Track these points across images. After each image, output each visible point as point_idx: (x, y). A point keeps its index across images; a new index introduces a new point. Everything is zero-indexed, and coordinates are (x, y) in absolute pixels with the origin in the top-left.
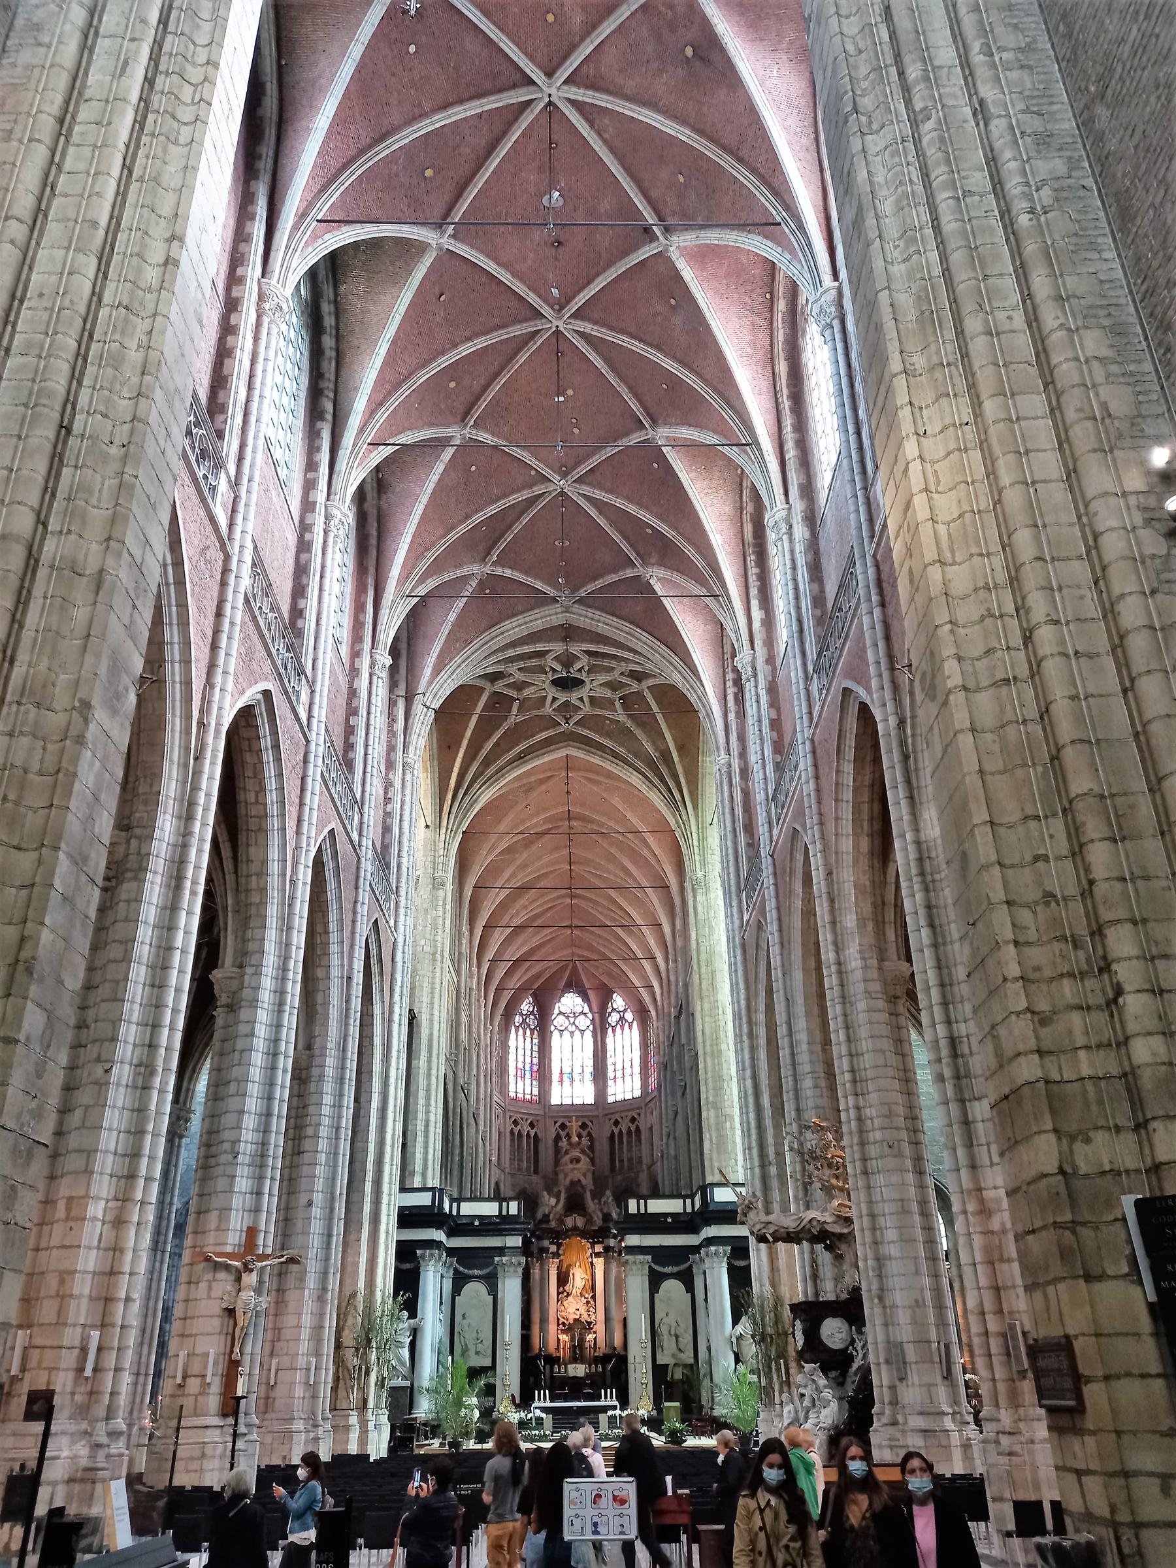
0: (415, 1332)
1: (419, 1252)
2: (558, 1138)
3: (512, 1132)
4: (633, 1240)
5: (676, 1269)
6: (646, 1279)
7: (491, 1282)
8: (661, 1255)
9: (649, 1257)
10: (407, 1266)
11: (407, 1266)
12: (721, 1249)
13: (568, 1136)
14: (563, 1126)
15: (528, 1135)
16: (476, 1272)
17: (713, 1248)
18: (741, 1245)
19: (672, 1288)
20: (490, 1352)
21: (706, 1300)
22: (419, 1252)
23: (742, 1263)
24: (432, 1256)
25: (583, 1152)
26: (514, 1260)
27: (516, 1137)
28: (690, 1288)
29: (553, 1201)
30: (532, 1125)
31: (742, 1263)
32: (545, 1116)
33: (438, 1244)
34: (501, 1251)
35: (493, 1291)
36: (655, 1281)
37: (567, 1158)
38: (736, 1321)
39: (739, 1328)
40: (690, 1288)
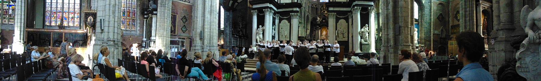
0: (264, 31)
1: (264, 10)
2: (321, 8)
3: (311, 7)
4: (331, 9)
5: (344, 17)
6: (335, 20)
7: (289, 21)
8: (338, 13)
9: (336, 13)
10: (261, 14)
11: (261, 14)
12: (358, 7)
13: (323, 8)
14: (322, 6)
15: (315, 7)
16: (285, 17)
17: (356, 7)
18: (365, 7)
19: (342, 22)
20: (289, 37)
21: (352, 24)
22: (264, 10)
23: (365, 13)
24: (268, 11)
25: (326, 10)
26: (295, 14)
27: (312, 8)
28: (348, 22)
29: (319, 19)
30: (316, 6)
31: (365, 13)
32: (318, 4)
33: (271, 8)
34: (293, 11)
35: (290, 22)
36: (337, 20)
37: (323, 11)
38: (361, 28)
39: (363, 30)
40: (348, 22)
